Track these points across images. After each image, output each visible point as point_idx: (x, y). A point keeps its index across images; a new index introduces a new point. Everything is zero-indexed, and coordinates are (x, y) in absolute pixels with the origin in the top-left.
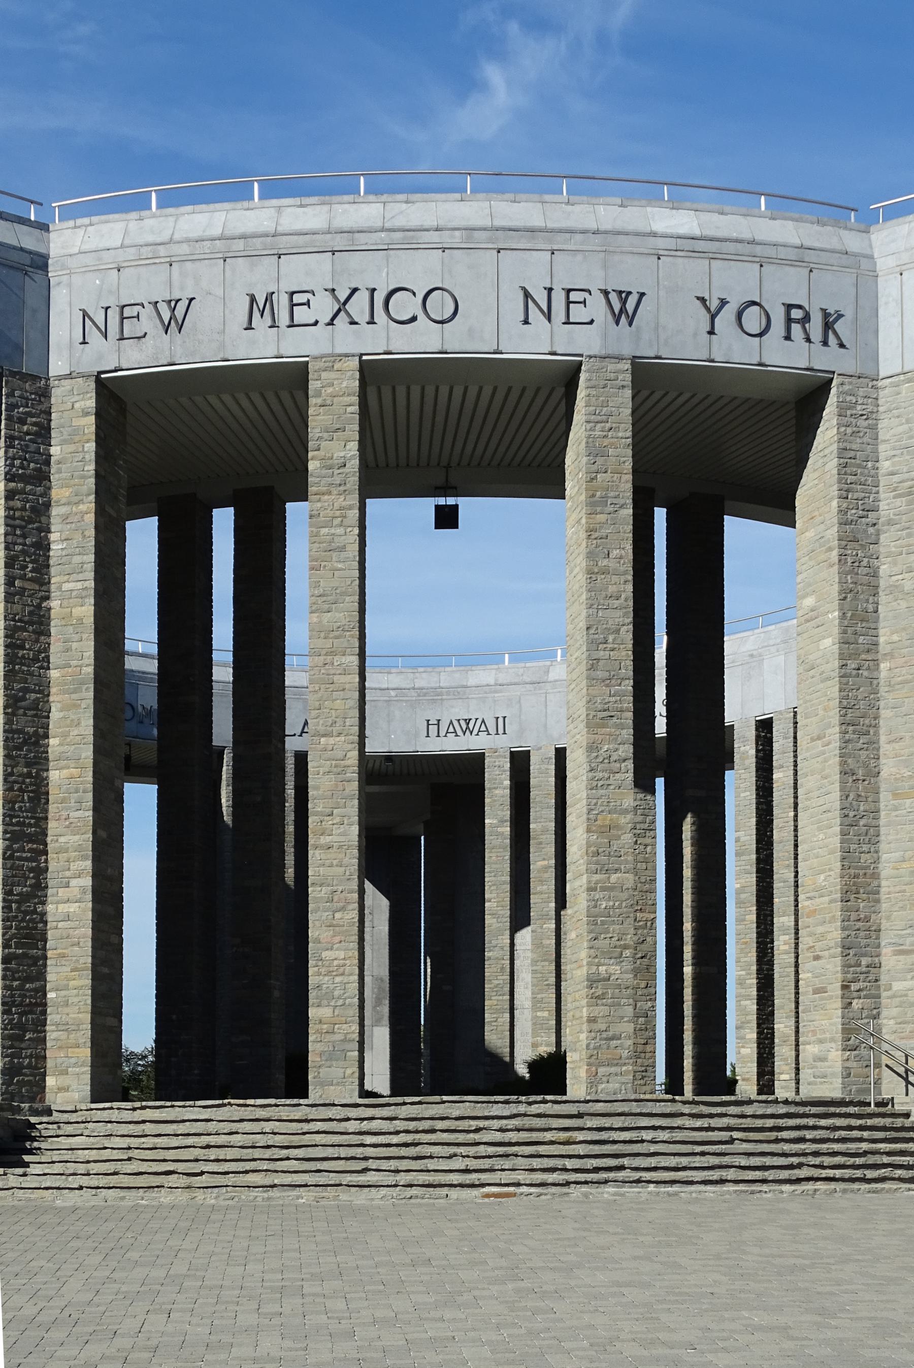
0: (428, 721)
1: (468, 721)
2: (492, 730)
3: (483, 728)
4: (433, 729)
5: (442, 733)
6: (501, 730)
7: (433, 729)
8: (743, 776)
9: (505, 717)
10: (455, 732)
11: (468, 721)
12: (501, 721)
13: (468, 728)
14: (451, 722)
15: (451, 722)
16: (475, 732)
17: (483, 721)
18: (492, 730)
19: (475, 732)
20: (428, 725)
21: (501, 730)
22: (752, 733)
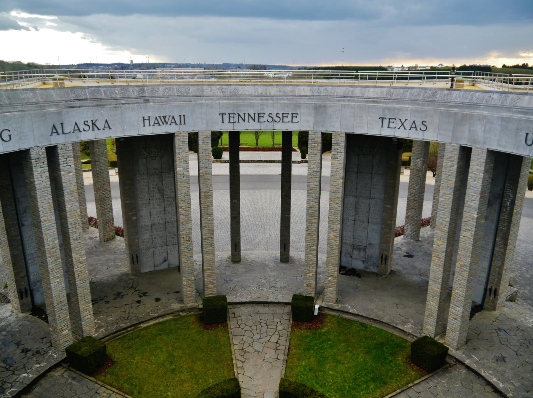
0: (144, 117)
1: (164, 117)
2: (178, 121)
3: (173, 121)
4: (147, 122)
5: (152, 124)
6: (183, 122)
7: (147, 122)
8: (313, 158)
9: (184, 116)
10: (158, 123)
11: (164, 117)
12: (182, 117)
13: (165, 121)
14: (156, 118)
15: (156, 118)
16: (169, 123)
17: (173, 117)
18: (178, 121)
19: (169, 123)
20: (144, 120)
21: (183, 122)
22: (319, 139)
